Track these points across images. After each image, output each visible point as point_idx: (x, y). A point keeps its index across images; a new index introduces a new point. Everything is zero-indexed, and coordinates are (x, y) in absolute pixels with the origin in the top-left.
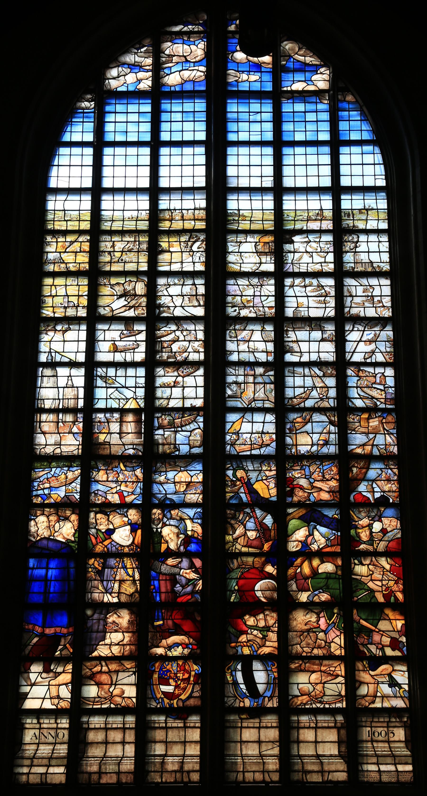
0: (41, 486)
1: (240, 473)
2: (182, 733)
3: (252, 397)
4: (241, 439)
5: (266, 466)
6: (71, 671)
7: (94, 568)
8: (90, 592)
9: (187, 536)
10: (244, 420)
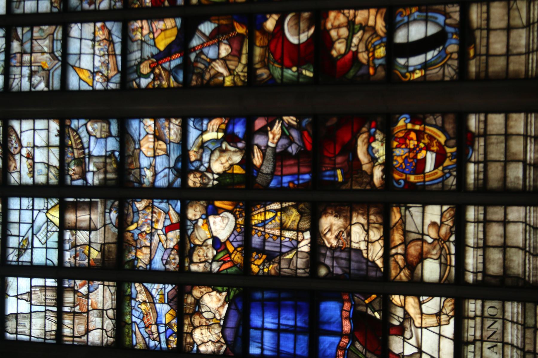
0: (155, 336)
1: (145, 69)
2: (493, 139)
3: (48, 55)
4: (101, 68)
5: (136, 35)
6: (402, 297)
7: (264, 265)
8: (296, 270)
9: (224, 139)
10: (77, 65)
